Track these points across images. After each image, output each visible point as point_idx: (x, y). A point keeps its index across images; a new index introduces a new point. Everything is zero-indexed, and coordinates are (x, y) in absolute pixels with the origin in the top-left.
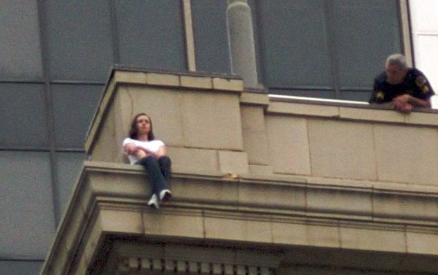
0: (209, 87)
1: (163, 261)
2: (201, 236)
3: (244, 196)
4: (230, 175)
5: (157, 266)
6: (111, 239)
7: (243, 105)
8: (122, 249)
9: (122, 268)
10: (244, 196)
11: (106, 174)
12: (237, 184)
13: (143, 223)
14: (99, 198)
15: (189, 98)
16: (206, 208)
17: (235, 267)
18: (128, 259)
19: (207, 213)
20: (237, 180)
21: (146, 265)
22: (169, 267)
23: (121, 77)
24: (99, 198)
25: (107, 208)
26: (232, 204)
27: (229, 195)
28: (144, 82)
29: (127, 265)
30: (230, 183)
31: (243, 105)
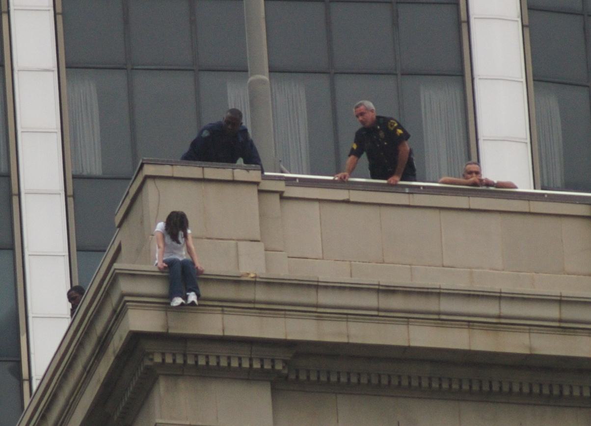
0: (230, 178)
1: (185, 355)
2: (220, 333)
3: (261, 294)
5: (180, 361)
6: (136, 337)
7: (260, 192)
9: (148, 363)
10: (261, 294)
11: (133, 275)
12: (254, 283)
13: (167, 321)
14: (127, 298)
15: (211, 189)
16: (226, 306)
17: (251, 359)
18: (152, 354)
19: (226, 311)
20: (254, 279)
21: (169, 360)
22: (190, 362)
23: (149, 170)
24: (127, 298)
26: (249, 302)
27: (246, 294)
29: (152, 360)
30: (248, 282)
31: (260, 192)
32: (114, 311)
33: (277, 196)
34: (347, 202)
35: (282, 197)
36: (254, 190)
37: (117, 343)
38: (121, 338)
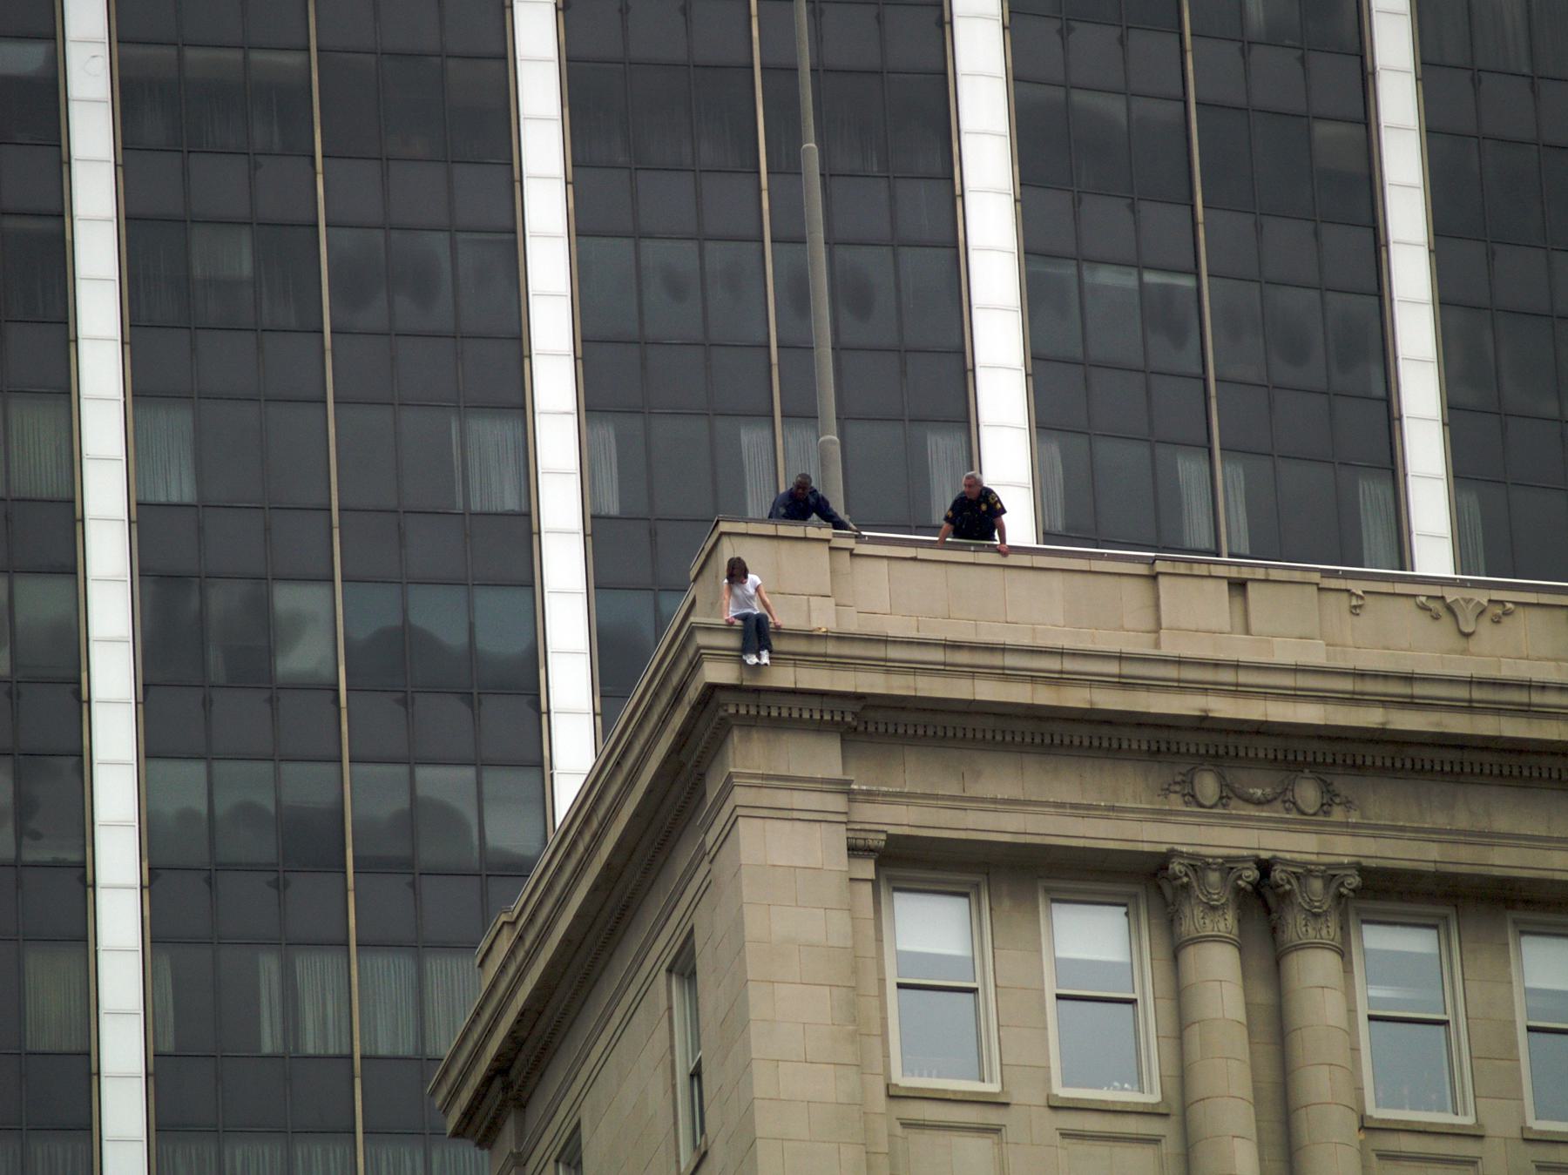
0: (802, 535)
2: (793, 686)
3: (831, 648)
4: (820, 629)
6: (712, 688)
8: (722, 697)
9: (722, 713)
10: (831, 648)
11: (709, 629)
12: (825, 637)
13: (741, 674)
14: (702, 651)
15: (785, 545)
16: (797, 659)
17: (821, 711)
18: (727, 705)
21: (743, 711)
22: (763, 713)
24: (702, 651)
25: (711, 660)
27: (818, 648)
28: (745, 532)
29: (726, 710)
30: (819, 636)
32: (690, 663)
33: (847, 554)
34: (914, 559)
35: (853, 555)
36: (825, 547)
37: (693, 694)
38: (696, 689)
